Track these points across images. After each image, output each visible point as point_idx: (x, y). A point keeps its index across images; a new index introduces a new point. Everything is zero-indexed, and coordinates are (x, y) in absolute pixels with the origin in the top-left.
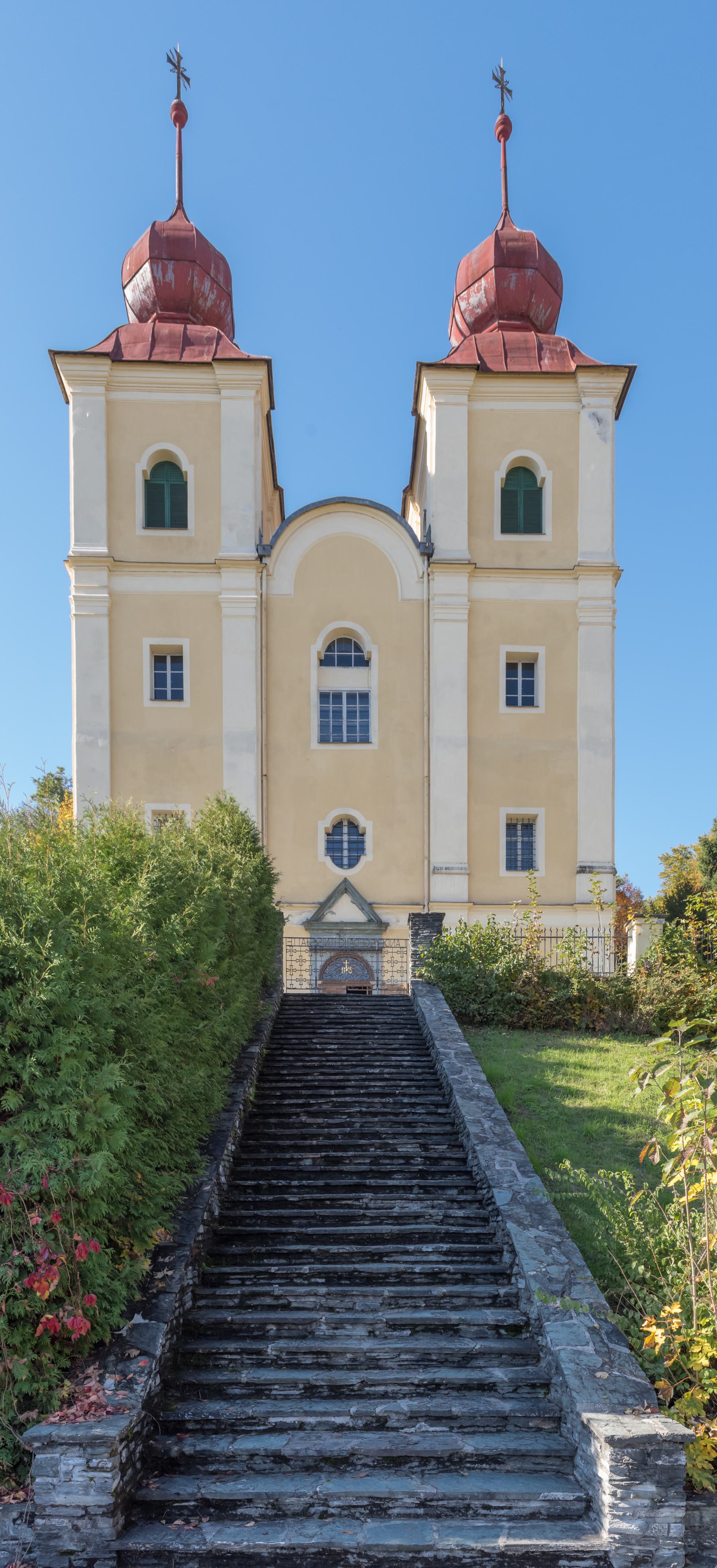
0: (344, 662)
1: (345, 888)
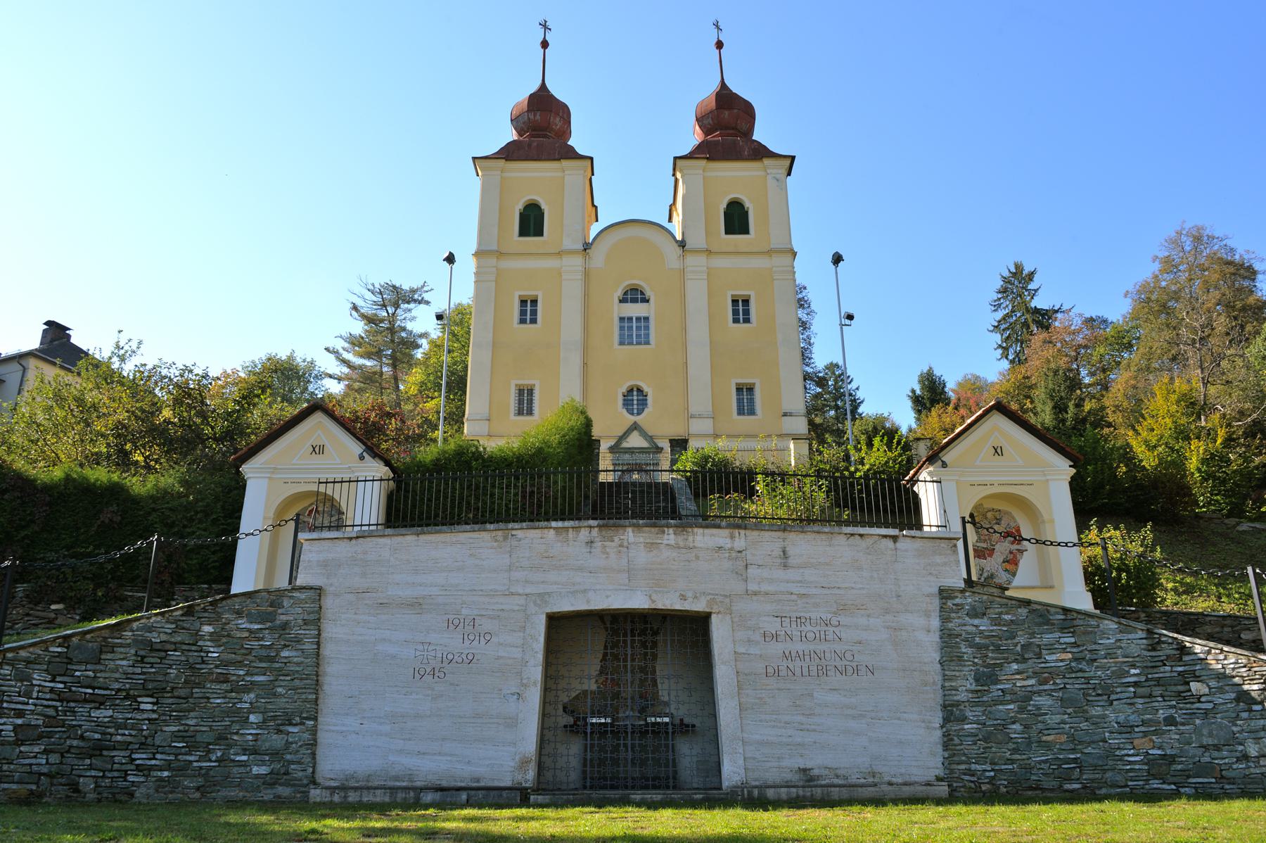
0: (634, 301)
1: (635, 427)
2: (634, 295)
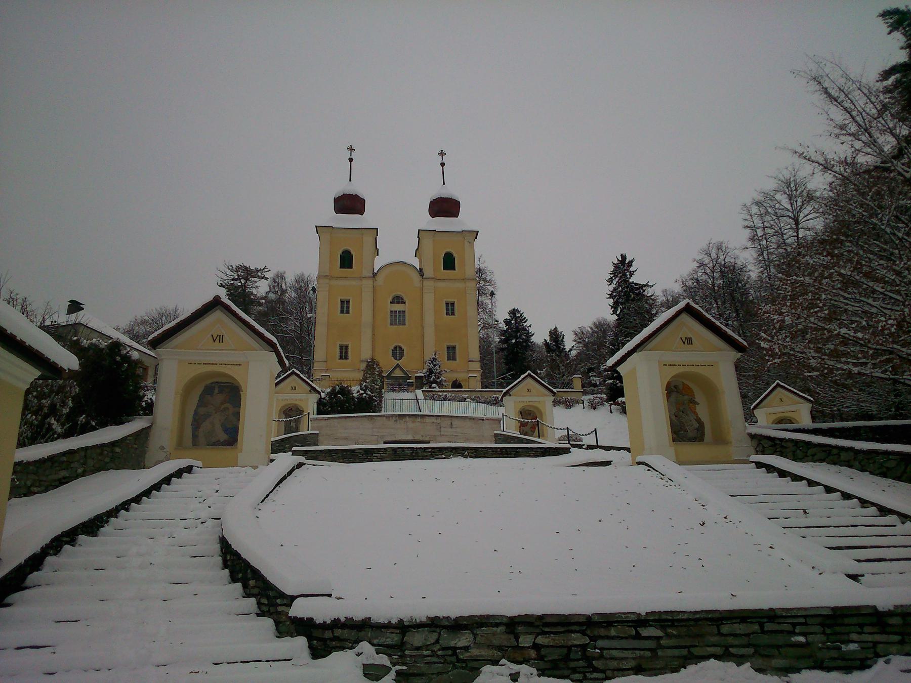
0: (398, 303)
2: (398, 300)
